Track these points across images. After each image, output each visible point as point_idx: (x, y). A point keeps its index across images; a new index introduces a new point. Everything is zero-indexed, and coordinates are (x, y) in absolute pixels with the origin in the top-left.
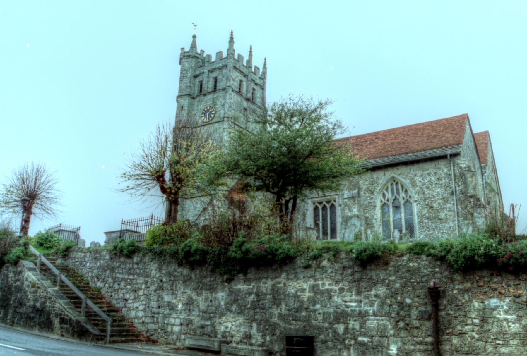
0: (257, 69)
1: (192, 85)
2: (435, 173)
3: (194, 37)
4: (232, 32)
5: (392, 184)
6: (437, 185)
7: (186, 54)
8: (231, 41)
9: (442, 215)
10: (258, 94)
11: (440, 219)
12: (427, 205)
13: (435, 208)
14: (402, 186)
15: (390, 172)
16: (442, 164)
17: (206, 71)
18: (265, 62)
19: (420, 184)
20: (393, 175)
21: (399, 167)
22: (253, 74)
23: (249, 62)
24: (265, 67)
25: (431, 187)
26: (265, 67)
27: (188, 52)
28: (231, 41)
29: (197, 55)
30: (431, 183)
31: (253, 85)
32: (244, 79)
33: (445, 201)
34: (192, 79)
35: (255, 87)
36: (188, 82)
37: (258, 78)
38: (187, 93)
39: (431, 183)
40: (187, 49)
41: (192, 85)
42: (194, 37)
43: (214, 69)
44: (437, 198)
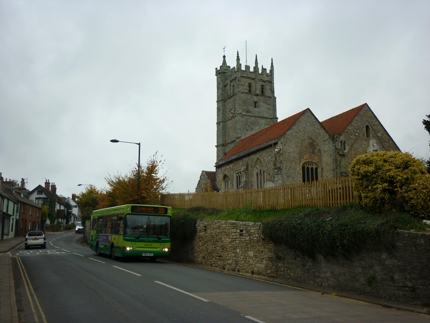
0: (264, 70)
1: (223, 93)
3: (224, 57)
4: (238, 52)
7: (219, 72)
8: (238, 59)
10: (267, 87)
17: (228, 82)
18: (272, 61)
22: (260, 75)
23: (256, 68)
24: (272, 66)
26: (272, 66)
27: (219, 70)
28: (238, 59)
32: (252, 81)
34: (224, 89)
35: (264, 84)
37: (265, 76)
40: (219, 69)
41: (223, 93)
42: (224, 57)
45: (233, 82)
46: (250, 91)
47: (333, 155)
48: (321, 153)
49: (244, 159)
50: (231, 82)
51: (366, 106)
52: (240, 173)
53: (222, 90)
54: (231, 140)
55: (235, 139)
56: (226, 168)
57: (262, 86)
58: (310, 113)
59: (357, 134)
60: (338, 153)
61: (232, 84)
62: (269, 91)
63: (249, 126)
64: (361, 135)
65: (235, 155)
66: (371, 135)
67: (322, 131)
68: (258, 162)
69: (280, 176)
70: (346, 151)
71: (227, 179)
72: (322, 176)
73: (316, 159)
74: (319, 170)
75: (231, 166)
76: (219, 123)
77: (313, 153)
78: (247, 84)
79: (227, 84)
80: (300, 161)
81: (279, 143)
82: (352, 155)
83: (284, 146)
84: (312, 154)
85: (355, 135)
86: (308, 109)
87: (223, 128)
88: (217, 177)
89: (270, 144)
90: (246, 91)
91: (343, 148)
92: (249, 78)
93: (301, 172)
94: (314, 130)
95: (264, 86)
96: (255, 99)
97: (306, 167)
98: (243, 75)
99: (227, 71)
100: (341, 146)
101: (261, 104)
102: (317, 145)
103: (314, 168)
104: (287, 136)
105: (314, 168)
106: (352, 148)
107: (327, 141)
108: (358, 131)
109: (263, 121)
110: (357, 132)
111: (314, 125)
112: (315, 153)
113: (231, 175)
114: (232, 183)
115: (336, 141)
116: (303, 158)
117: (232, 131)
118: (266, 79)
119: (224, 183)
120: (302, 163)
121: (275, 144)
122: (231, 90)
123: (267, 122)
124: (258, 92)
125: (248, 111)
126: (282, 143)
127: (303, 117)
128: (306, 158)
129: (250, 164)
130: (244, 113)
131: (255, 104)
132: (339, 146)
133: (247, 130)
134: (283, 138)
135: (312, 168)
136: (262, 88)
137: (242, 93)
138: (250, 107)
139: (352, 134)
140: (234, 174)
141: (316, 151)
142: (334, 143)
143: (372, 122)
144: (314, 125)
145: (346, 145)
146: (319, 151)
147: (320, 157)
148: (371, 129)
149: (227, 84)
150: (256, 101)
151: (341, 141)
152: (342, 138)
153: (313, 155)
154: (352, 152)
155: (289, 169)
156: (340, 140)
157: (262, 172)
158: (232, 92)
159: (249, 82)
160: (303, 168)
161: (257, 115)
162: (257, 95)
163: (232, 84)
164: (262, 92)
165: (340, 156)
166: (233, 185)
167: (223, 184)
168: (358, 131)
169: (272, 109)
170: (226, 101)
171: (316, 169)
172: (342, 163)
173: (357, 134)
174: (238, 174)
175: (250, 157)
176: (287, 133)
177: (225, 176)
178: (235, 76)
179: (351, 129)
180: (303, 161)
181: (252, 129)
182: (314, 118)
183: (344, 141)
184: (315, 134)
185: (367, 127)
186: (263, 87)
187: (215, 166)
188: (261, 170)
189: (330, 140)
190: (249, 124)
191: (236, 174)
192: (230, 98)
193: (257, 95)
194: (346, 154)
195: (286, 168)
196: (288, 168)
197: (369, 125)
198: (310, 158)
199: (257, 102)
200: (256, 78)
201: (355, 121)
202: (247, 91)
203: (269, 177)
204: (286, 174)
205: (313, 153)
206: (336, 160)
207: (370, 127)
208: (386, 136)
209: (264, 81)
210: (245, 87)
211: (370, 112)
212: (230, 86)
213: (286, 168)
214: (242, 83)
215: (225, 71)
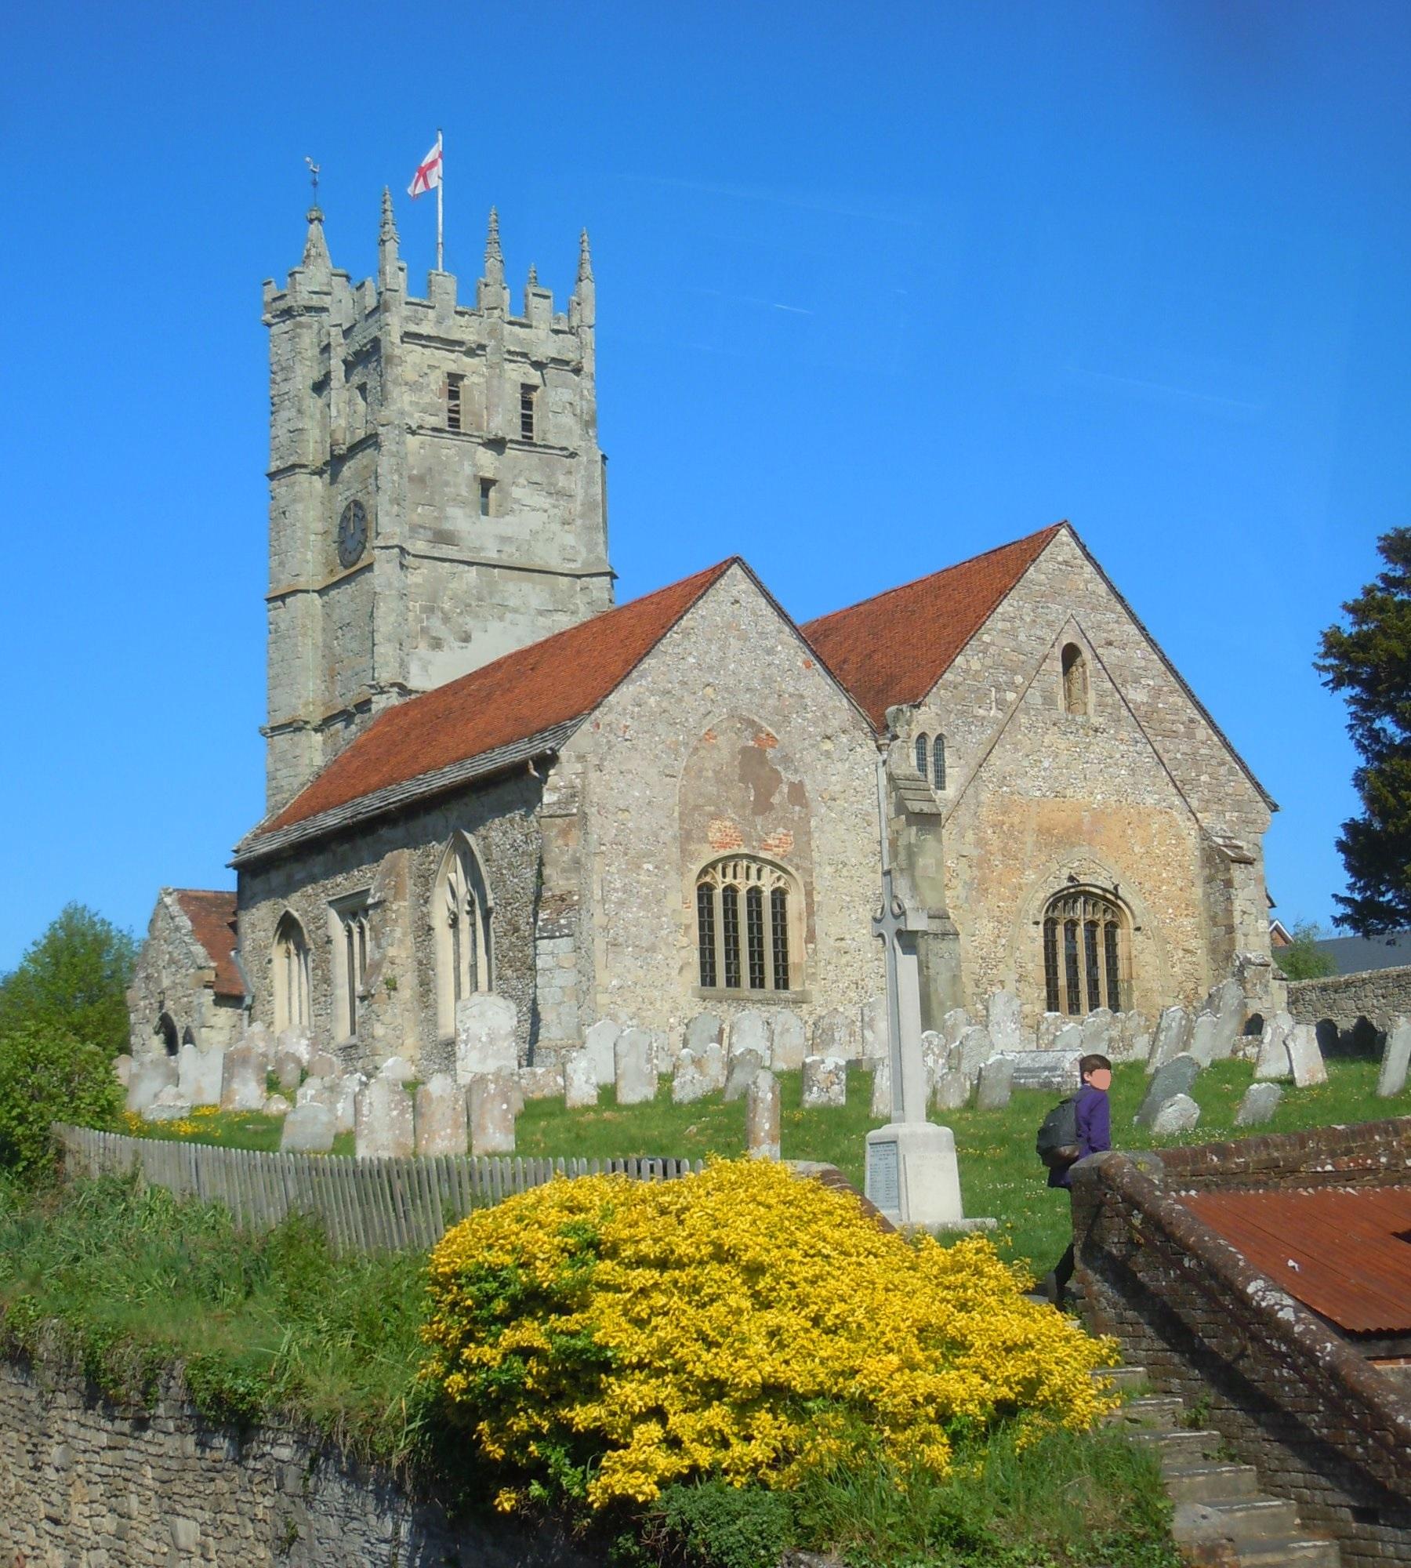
7: (282, 305)
21: (466, 800)
31: (519, 373)
35: (535, 377)
36: (293, 413)
43: (356, 354)
46: (454, 422)
47: (875, 819)
48: (805, 805)
49: (385, 832)
50: (349, 367)
51: (1063, 531)
56: (290, 876)
57: (527, 388)
58: (745, 585)
59: (1011, 696)
60: (900, 808)
62: (567, 420)
63: (446, 619)
64: (1035, 697)
65: (341, 803)
66: (1092, 697)
67: (818, 687)
69: (564, 944)
70: (950, 791)
72: (811, 937)
73: (777, 843)
74: (794, 903)
76: (282, 598)
77: (763, 806)
78: (437, 381)
80: (686, 855)
81: (563, 753)
82: (984, 811)
83: (593, 776)
84: (755, 813)
85: (1001, 704)
89: (518, 757)
90: (432, 421)
91: (931, 776)
92: (450, 344)
93: (692, 916)
94: (767, 680)
95: (535, 388)
96: (487, 462)
97: (718, 893)
98: (413, 328)
99: (326, 301)
100: (922, 766)
101: (517, 492)
102: (787, 760)
103: (767, 893)
105: (767, 893)
106: (985, 775)
107: (844, 739)
108: (1019, 679)
109: (526, 587)
110: (1012, 686)
111: (770, 651)
112: (771, 807)
115: (895, 737)
116: (704, 839)
118: (548, 348)
120: (696, 868)
121: (547, 761)
123: (553, 593)
124: (504, 421)
125: (443, 537)
126: (581, 758)
127: (704, 608)
128: (720, 836)
130: (420, 546)
131: (485, 493)
132: (906, 761)
133: (437, 644)
134: (586, 726)
135: (754, 894)
136: (527, 404)
137: (413, 433)
138: (454, 512)
139: (981, 698)
141: (775, 800)
142: (879, 749)
143: (1098, 627)
144: (770, 651)
145: (949, 758)
146: (797, 793)
147: (803, 833)
148: (1091, 665)
150: (488, 474)
151: (922, 736)
152: (926, 718)
153: (759, 820)
154: (985, 796)
155: (621, 904)
156: (915, 735)
159: (453, 368)
160: (705, 892)
161: (492, 555)
162: (497, 445)
164: (527, 424)
165: (909, 823)
168: (1019, 679)
169: (579, 522)
171: (779, 896)
172: (921, 862)
173: (1011, 696)
180: (709, 855)
181: (466, 638)
182: (769, 611)
183: (940, 738)
184: (772, 702)
185: (1070, 654)
186: (535, 396)
187: (237, 866)
189: (859, 734)
190: (447, 606)
193: (497, 445)
194: (944, 813)
195: (604, 901)
196: (614, 897)
197: (1083, 646)
198: (746, 838)
199: (493, 482)
200: (491, 344)
201: (1000, 625)
204: (606, 929)
205: (763, 806)
206: (893, 844)
207: (1087, 654)
208: (1179, 700)
209: (538, 365)
210: (427, 399)
211: (1089, 569)
213: (604, 901)
214: (411, 376)
215: (316, 301)
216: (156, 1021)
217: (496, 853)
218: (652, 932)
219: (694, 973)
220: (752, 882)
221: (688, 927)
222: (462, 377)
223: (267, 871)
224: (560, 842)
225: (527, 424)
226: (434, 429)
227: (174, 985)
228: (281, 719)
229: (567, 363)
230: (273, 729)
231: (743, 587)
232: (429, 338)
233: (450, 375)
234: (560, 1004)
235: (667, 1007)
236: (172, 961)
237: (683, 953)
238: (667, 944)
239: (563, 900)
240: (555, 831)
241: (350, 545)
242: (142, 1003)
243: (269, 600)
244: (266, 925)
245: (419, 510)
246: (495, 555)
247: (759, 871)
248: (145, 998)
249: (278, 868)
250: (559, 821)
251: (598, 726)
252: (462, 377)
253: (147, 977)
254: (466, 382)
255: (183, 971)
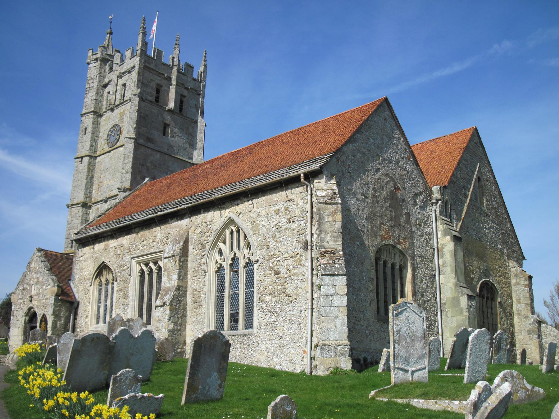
0: (189, 68)
2: (286, 209)
5: (232, 233)
6: (287, 232)
9: (290, 288)
11: (288, 295)
12: (272, 269)
13: (281, 275)
14: (245, 236)
15: (228, 211)
16: (296, 192)
19: (265, 231)
20: (231, 215)
22: (181, 75)
25: (278, 235)
29: (108, 57)
30: (278, 227)
33: (296, 262)
34: (100, 90)
35: (185, 93)
36: (94, 94)
37: (189, 79)
38: (93, 109)
39: (278, 227)
43: (123, 73)
44: (286, 255)
45: (126, 77)
52: (155, 263)
53: (97, 93)
54: (105, 195)
55: (116, 192)
57: (183, 96)
61: (121, 82)
63: (148, 169)
68: (227, 232)
71: (106, 276)
75: (125, 240)
78: (153, 85)
79: (110, 81)
86: (386, 100)
87: (89, 169)
88: (76, 268)
90: (150, 98)
95: (185, 97)
104: (344, 158)
113: (122, 266)
114: (124, 290)
117: (110, 176)
119: (97, 287)
122: (118, 93)
129: (193, 238)
130: (141, 141)
131: (165, 128)
136: (182, 102)
140: (134, 262)
149: (110, 81)
157: (242, 262)
158: (118, 97)
159: (159, 82)
163: (121, 82)
164: (181, 109)
166: (126, 297)
167: (94, 290)
170: (101, 116)
174: (147, 265)
175: (199, 219)
176: (345, 149)
177: (102, 268)
178: (132, 65)
179: (459, 177)
186: (185, 100)
188: (235, 259)
190: (149, 165)
191: (139, 263)
192: (112, 110)
202: (153, 99)
203: (273, 283)
210: (149, 90)
212: (117, 85)
214: (145, 82)
216: (26, 310)
217: (263, 231)
218: (359, 281)
219: (374, 306)
220: (393, 260)
221: (373, 279)
222: (161, 86)
223: (94, 244)
224: (330, 219)
225: (181, 109)
226: (151, 102)
227: (38, 294)
228: (76, 202)
229: (196, 91)
230: (72, 205)
231: (387, 113)
232: (153, 69)
233: (158, 85)
234: (336, 317)
235: (365, 324)
236: (37, 283)
237: (371, 294)
238: (365, 288)
239: (334, 254)
240: (327, 212)
241: (112, 139)
242: (19, 301)
243: (75, 158)
244: (90, 268)
245: (142, 128)
246: (166, 151)
247: (394, 255)
248: (21, 299)
249: (100, 242)
250: (329, 206)
251: (338, 161)
252: (161, 86)
253: (24, 289)
254: (163, 89)
255: (44, 287)
